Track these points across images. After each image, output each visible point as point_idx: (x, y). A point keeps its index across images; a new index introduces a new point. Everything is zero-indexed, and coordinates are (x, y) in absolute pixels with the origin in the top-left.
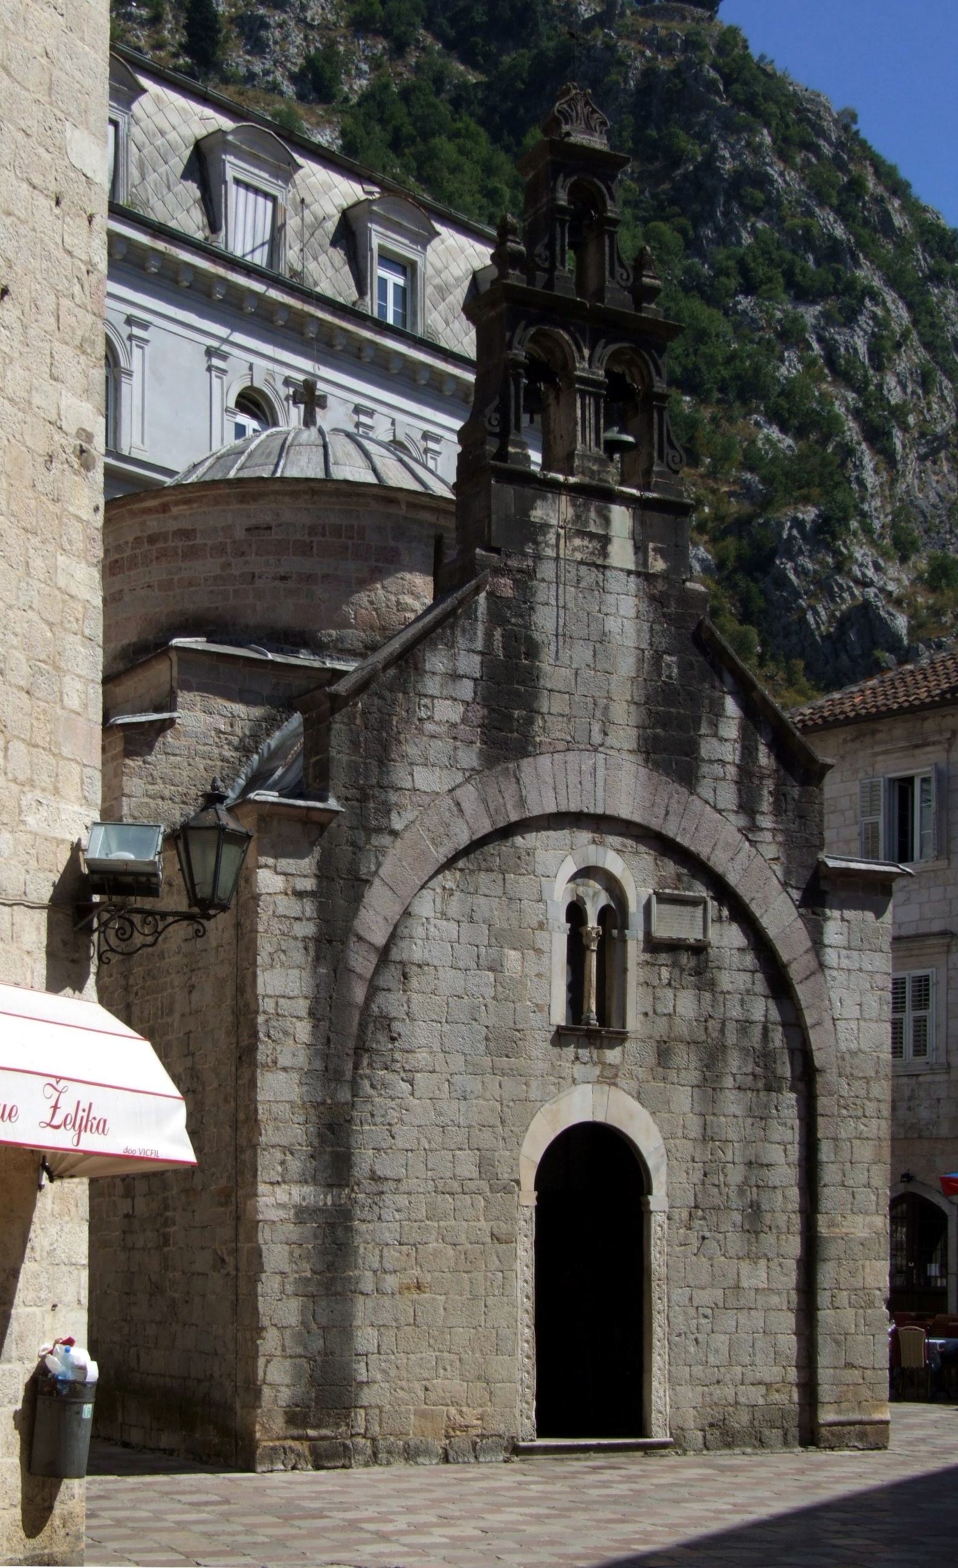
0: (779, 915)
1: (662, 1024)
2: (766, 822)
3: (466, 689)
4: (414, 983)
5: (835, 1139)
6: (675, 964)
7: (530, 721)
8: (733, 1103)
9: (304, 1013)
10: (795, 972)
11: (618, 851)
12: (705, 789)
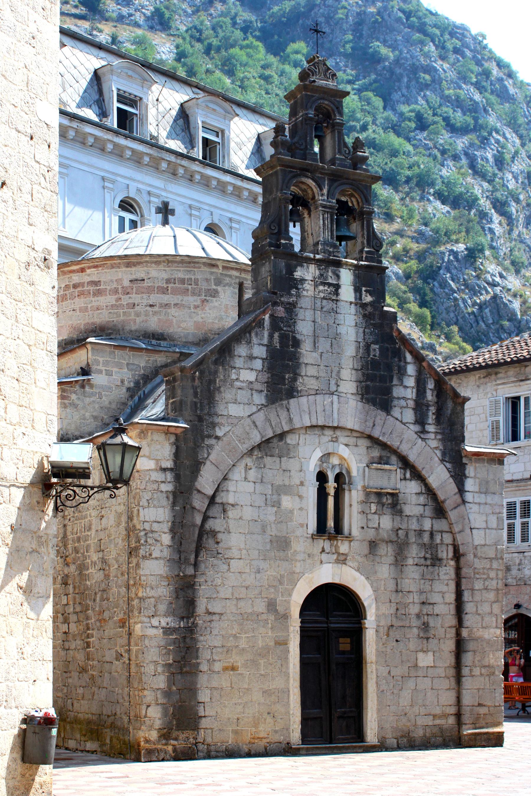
2: (431, 428)
3: (258, 364)
5: (473, 590)
7: (295, 380)
8: (412, 575)
10: (448, 505)
11: (346, 445)
12: (396, 412)
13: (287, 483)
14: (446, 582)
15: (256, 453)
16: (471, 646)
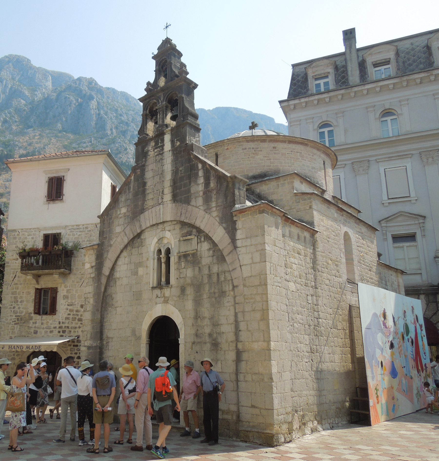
1: (182, 281)
2: (214, 204)
4: (118, 283)
5: (243, 312)
9: (92, 296)
10: (225, 253)
11: (169, 231)
12: (193, 203)
13: (141, 261)
14: (228, 308)
15: (128, 248)
16: (245, 356)
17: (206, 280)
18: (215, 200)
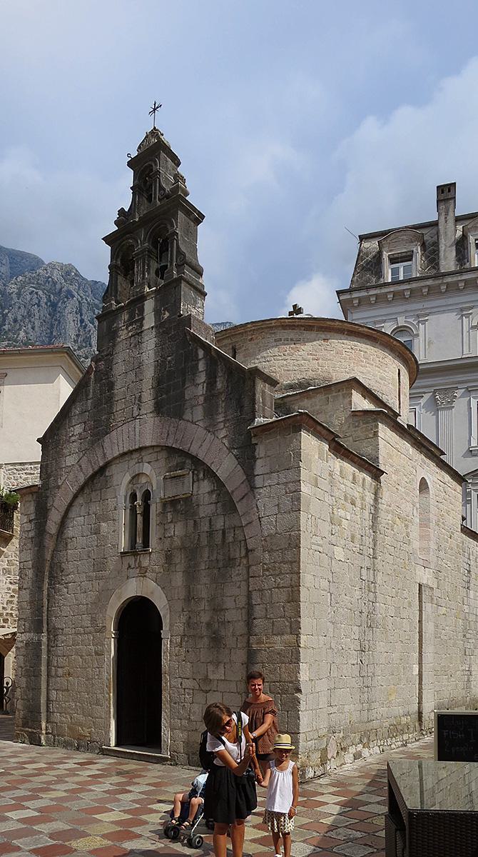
0: (226, 466)
6: (175, 510)
11: (149, 463)
12: (188, 416)
17: (204, 541)
18: (223, 410)
